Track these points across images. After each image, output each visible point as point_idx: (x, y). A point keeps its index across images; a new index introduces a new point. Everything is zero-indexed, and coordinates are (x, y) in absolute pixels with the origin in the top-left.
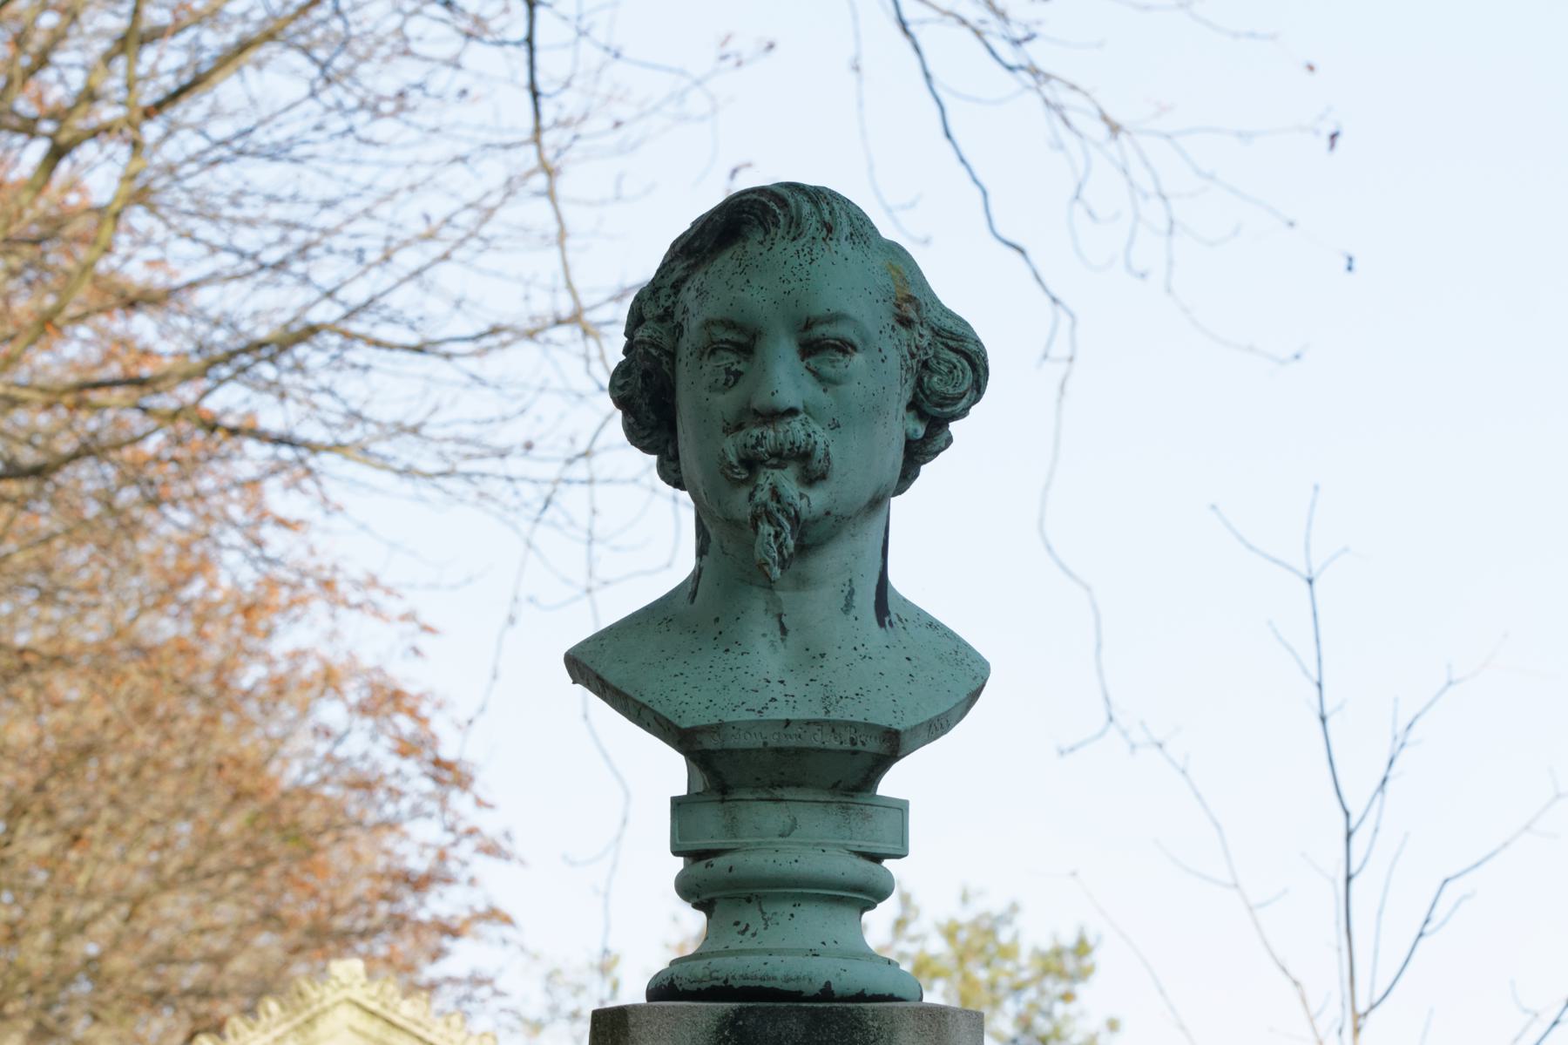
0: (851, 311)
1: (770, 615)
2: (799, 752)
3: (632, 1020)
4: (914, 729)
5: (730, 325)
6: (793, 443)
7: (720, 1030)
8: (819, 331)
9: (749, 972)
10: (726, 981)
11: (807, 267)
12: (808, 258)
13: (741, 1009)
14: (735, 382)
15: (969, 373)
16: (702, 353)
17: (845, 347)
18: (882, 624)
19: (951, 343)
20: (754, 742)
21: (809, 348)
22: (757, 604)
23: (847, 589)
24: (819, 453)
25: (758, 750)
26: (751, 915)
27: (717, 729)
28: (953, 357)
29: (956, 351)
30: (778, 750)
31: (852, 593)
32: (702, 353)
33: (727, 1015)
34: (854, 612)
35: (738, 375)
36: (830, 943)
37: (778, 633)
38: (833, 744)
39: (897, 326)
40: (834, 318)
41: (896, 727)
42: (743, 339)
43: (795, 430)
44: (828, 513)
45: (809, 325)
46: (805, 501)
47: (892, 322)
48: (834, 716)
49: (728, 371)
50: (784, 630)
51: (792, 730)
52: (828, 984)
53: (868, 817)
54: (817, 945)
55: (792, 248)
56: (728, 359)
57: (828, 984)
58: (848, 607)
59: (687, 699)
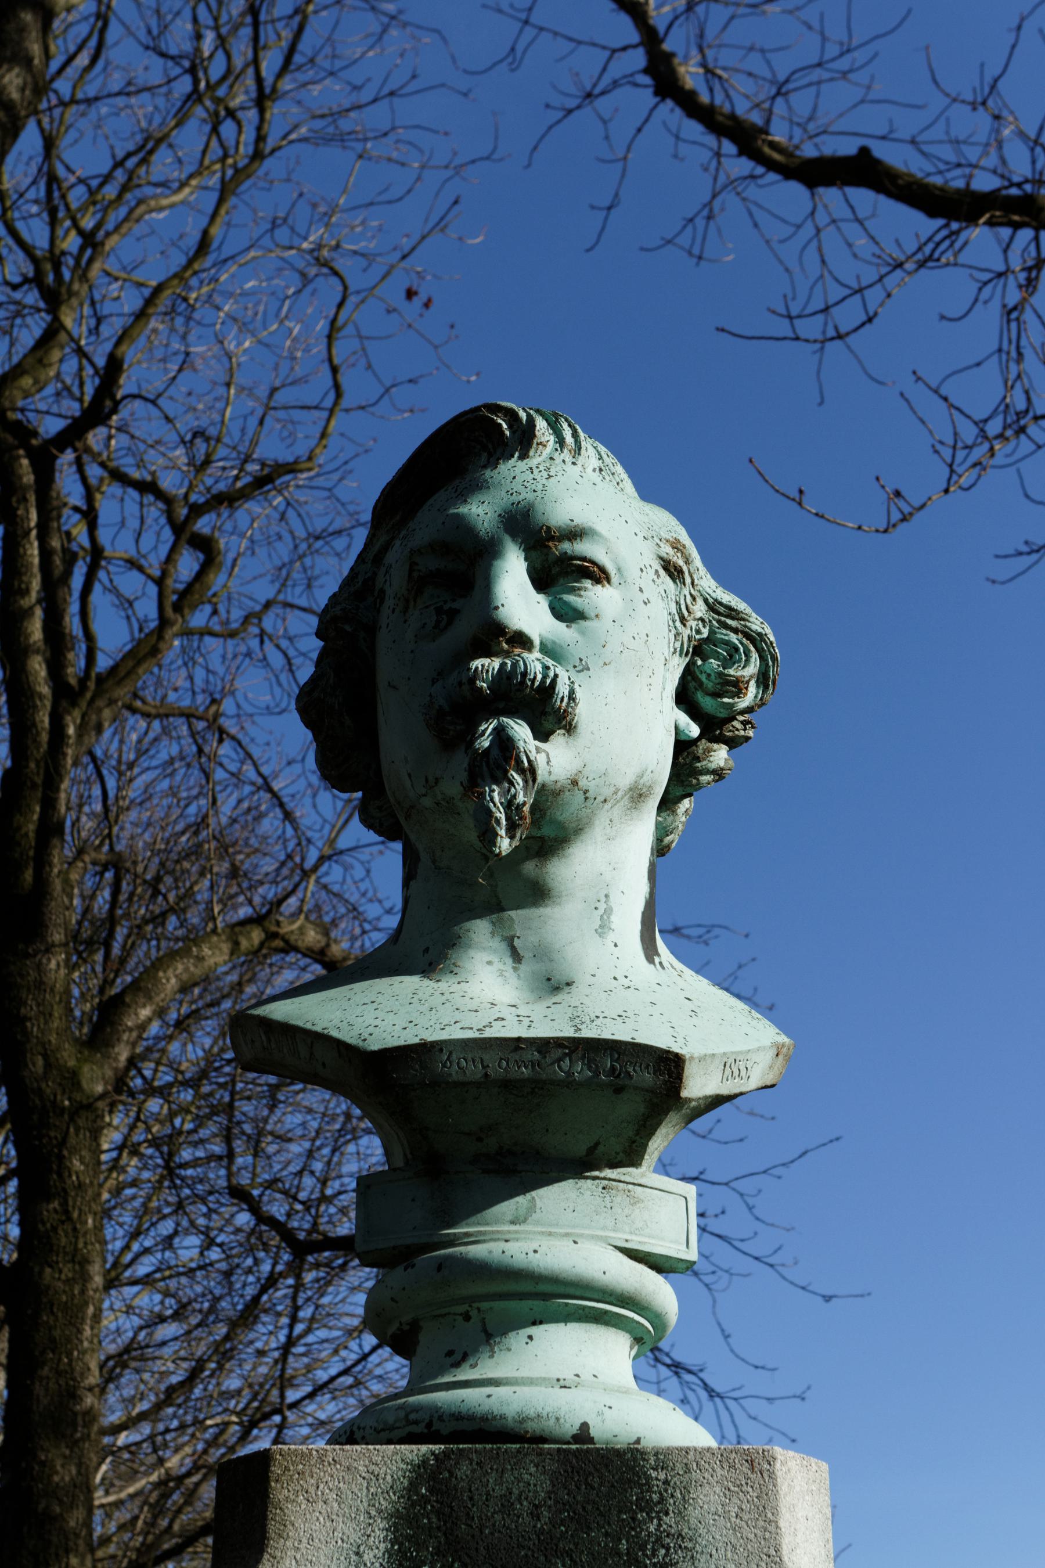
0: (600, 527)
1: (497, 939)
3: (276, 1470)
4: (702, 1059)
6: (525, 674)
9: (464, 1409)
10: (429, 1425)
11: (544, 481)
12: (545, 474)
13: (446, 1454)
14: (450, 623)
15: (755, 655)
16: (407, 601)
18: (650, 959)
19: (729, 622)
20: (474, 1072)
22: (480, 929)
23: (602, 906)
24: (562, 689)
25: (478, 1085)
28: (734, 638)
29: (735, 631)
30: (507, 1084)
31: (608, 911)
32: (407, 601)
33: (424, 1462)
34: (611, 937)
35: (453, 614)
36: (586, 1376)
37: (509, 961)
39: (662, 572)
40: (576, 534)
41: (676, 1049)
44: (575, 783)
46: (543, 755)
47: (657, 565)
48: (587, 1033)
49: (439, 611)
52: (585, 1426)
53: (635, 1201)
54: (568, 1375)
57: (585, 1426)
58: (603, 928)
59: (377, 1022)
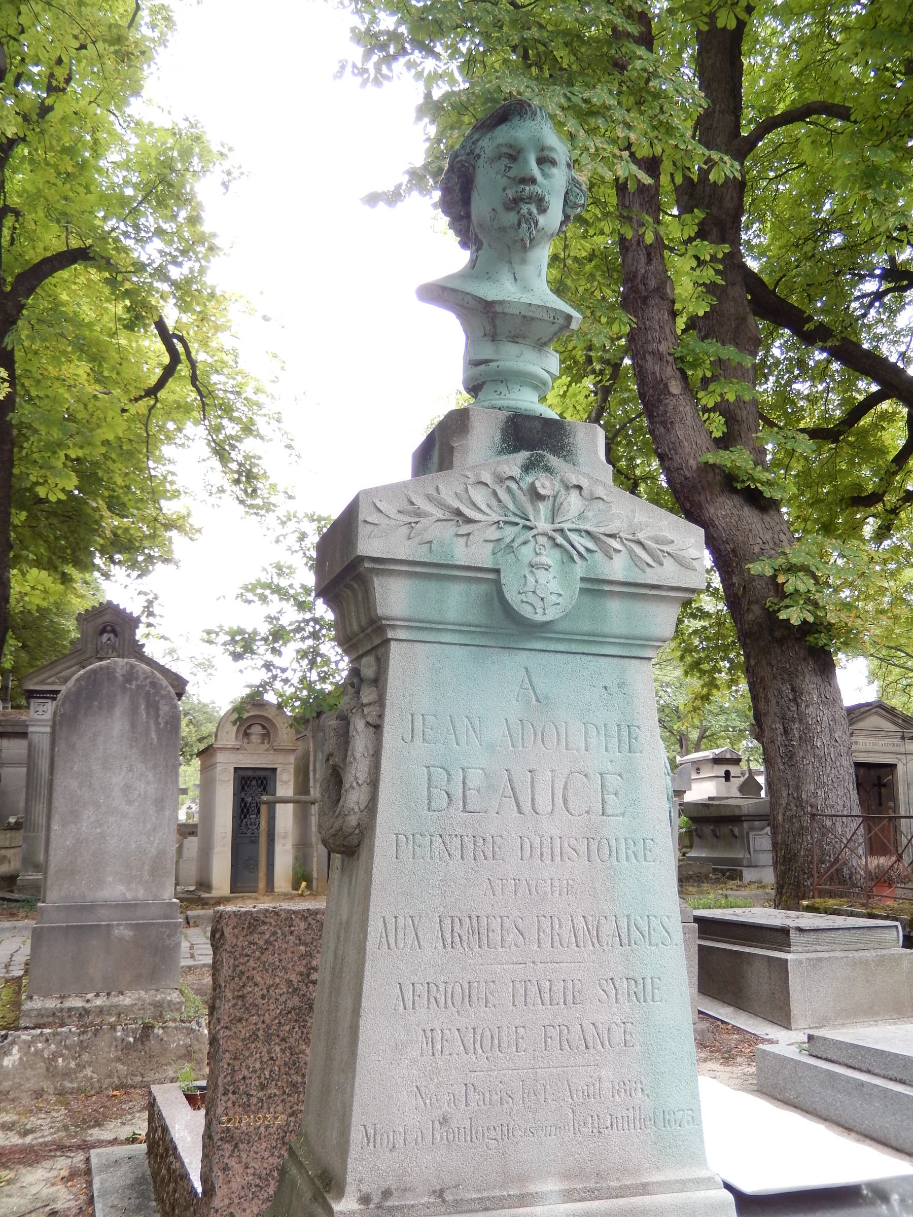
2: (533, 319)
5: (511, 146)
7: (507, 422)
8: (546, 153)
17: (553, 163)
21: (541, 161)
26: (502, 388)
27: (501, 303)
30: (524, 317)
38: (546, 317)
42: (514, 153)
43: (537, 189)
45: (543, 149)
50: (515, 279)
51: (532, 308)
55: (533, 123)
56: (505, 161)
